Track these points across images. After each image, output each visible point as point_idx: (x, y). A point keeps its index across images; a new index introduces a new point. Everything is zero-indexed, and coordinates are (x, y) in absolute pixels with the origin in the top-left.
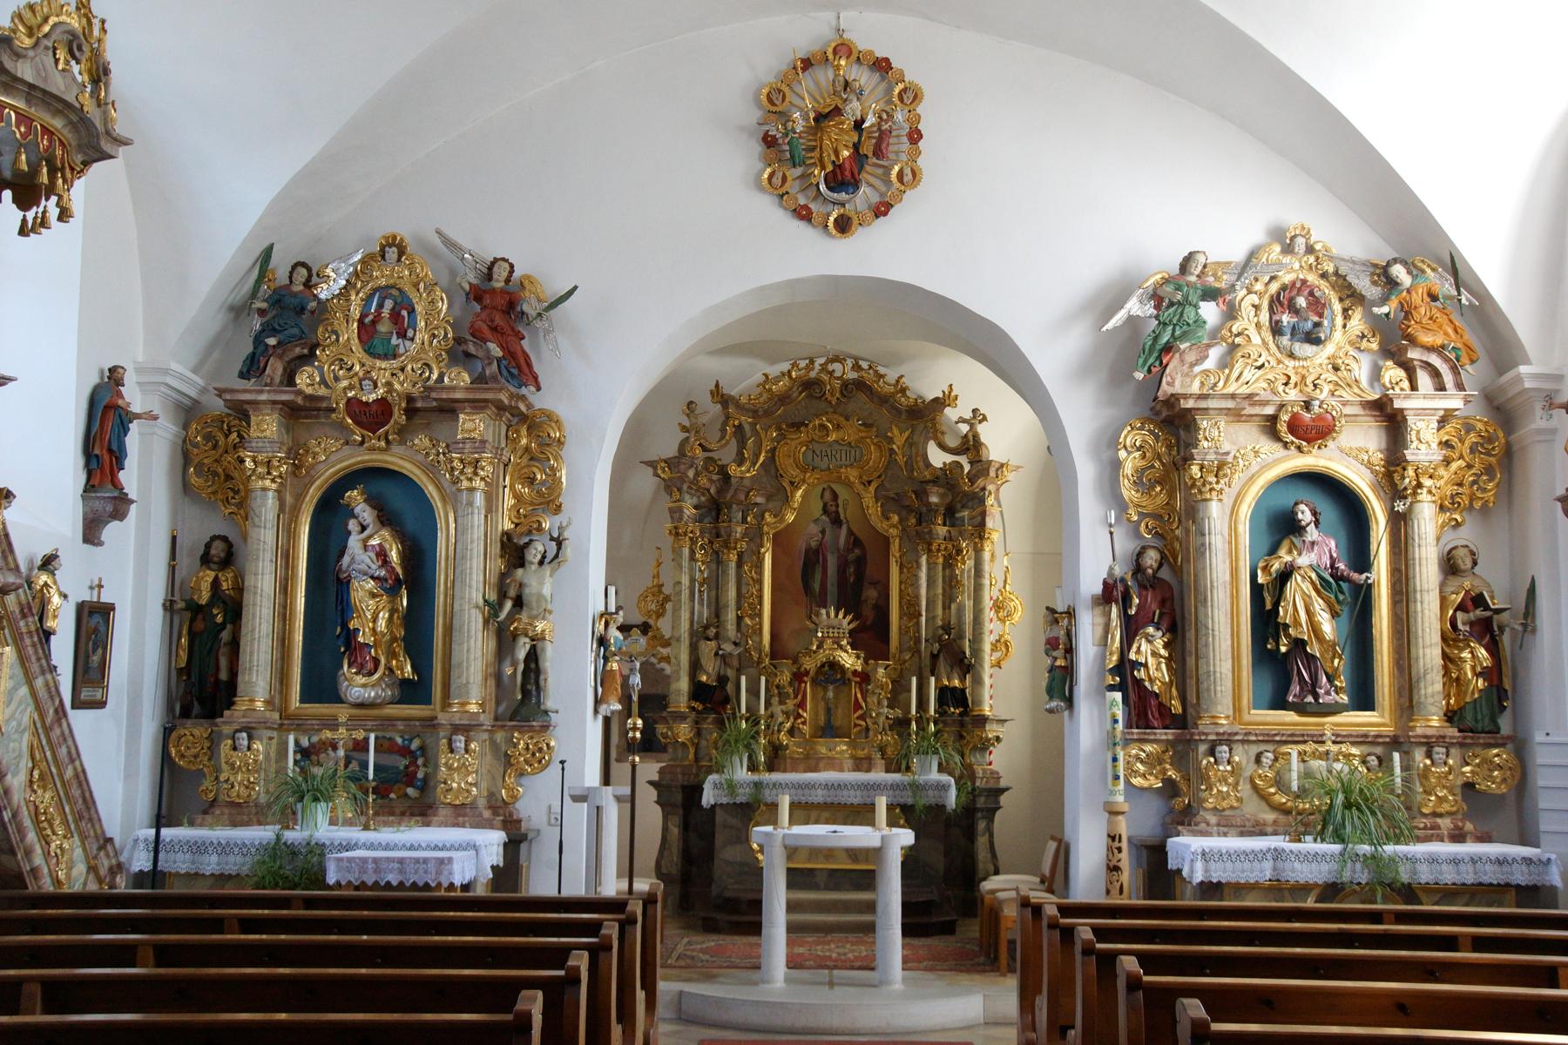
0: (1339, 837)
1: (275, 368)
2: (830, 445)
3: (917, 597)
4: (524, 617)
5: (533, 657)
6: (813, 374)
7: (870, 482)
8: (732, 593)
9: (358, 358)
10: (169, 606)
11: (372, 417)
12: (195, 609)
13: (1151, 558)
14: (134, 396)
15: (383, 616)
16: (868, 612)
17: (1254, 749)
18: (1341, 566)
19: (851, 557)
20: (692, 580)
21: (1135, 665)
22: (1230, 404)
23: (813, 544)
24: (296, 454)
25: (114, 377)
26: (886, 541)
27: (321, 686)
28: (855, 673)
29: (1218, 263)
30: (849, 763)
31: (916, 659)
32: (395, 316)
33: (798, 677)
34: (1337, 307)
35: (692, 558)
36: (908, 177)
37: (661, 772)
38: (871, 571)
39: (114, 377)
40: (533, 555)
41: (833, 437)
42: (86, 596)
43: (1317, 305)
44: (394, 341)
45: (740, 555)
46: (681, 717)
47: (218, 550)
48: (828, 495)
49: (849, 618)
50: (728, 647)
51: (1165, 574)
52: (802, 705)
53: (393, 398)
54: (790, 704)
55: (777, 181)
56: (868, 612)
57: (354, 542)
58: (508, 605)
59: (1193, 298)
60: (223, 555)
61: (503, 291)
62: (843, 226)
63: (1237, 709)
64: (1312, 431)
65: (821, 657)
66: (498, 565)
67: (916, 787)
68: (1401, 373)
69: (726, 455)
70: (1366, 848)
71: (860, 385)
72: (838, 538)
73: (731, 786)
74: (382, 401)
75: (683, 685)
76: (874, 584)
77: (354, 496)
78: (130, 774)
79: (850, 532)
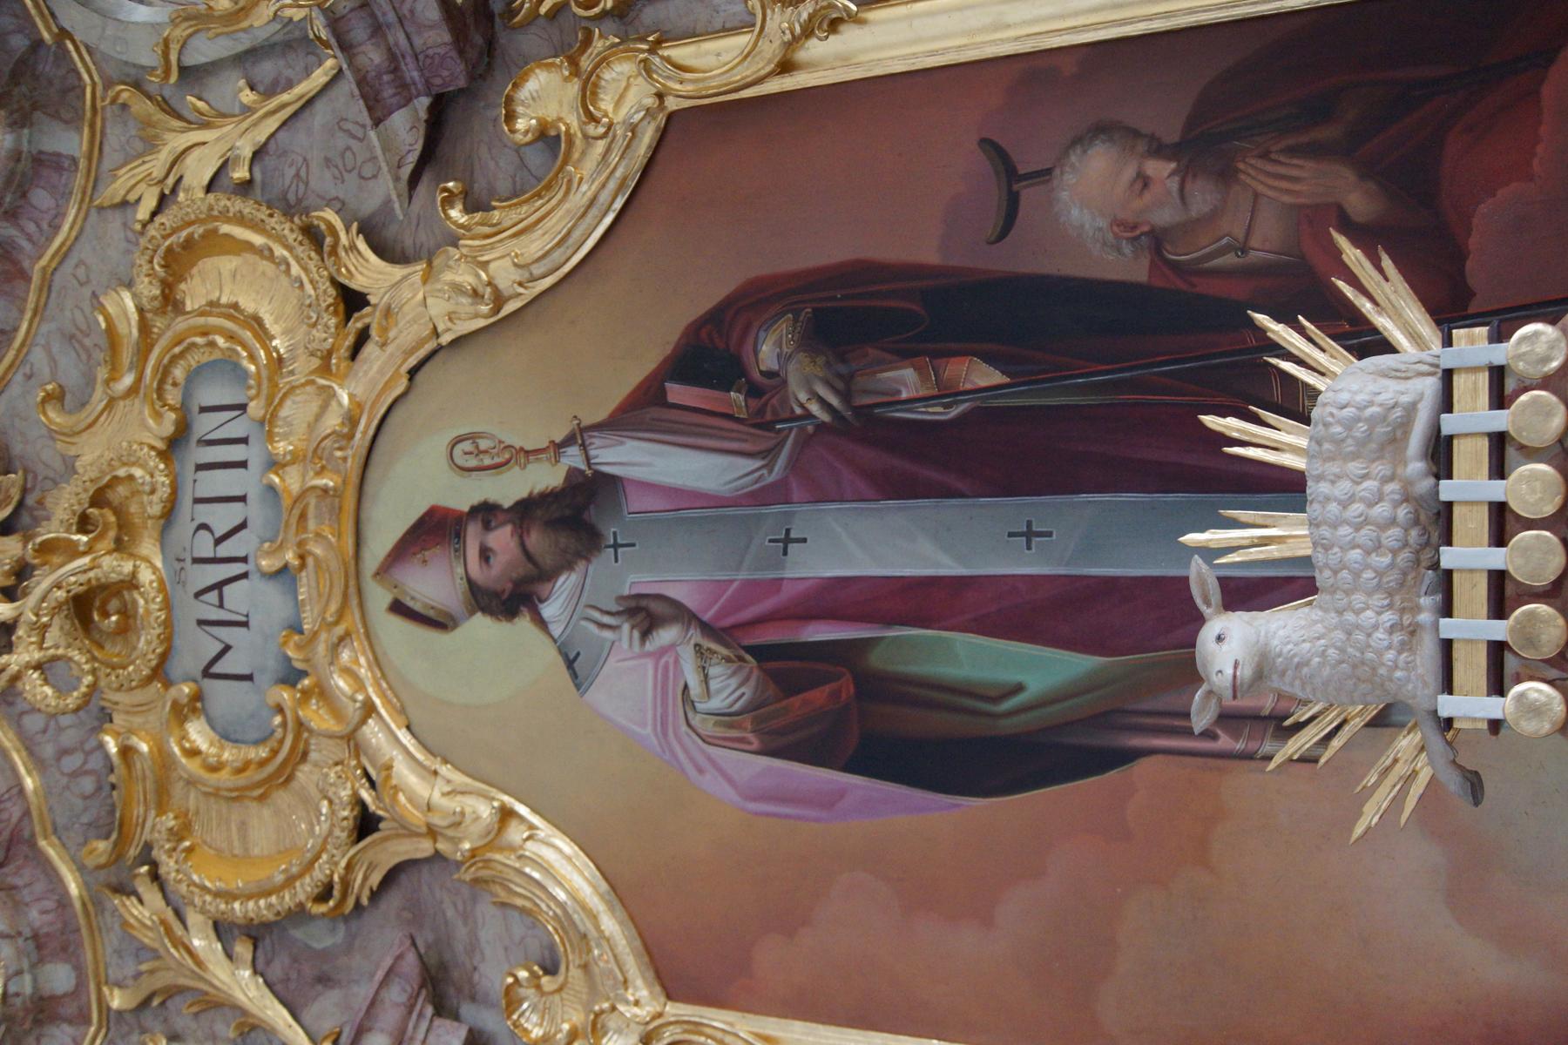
2: (178, 563)
7: (352, 301)
19: (810, 393)
23: (726, 687)
26: (688, 131)
38: (913, 224)
41: (148, 566)
48: (433, 582)
49: (1299, 345)
72: (685, 499)
76: (1013, 181)
79: (642, 411)
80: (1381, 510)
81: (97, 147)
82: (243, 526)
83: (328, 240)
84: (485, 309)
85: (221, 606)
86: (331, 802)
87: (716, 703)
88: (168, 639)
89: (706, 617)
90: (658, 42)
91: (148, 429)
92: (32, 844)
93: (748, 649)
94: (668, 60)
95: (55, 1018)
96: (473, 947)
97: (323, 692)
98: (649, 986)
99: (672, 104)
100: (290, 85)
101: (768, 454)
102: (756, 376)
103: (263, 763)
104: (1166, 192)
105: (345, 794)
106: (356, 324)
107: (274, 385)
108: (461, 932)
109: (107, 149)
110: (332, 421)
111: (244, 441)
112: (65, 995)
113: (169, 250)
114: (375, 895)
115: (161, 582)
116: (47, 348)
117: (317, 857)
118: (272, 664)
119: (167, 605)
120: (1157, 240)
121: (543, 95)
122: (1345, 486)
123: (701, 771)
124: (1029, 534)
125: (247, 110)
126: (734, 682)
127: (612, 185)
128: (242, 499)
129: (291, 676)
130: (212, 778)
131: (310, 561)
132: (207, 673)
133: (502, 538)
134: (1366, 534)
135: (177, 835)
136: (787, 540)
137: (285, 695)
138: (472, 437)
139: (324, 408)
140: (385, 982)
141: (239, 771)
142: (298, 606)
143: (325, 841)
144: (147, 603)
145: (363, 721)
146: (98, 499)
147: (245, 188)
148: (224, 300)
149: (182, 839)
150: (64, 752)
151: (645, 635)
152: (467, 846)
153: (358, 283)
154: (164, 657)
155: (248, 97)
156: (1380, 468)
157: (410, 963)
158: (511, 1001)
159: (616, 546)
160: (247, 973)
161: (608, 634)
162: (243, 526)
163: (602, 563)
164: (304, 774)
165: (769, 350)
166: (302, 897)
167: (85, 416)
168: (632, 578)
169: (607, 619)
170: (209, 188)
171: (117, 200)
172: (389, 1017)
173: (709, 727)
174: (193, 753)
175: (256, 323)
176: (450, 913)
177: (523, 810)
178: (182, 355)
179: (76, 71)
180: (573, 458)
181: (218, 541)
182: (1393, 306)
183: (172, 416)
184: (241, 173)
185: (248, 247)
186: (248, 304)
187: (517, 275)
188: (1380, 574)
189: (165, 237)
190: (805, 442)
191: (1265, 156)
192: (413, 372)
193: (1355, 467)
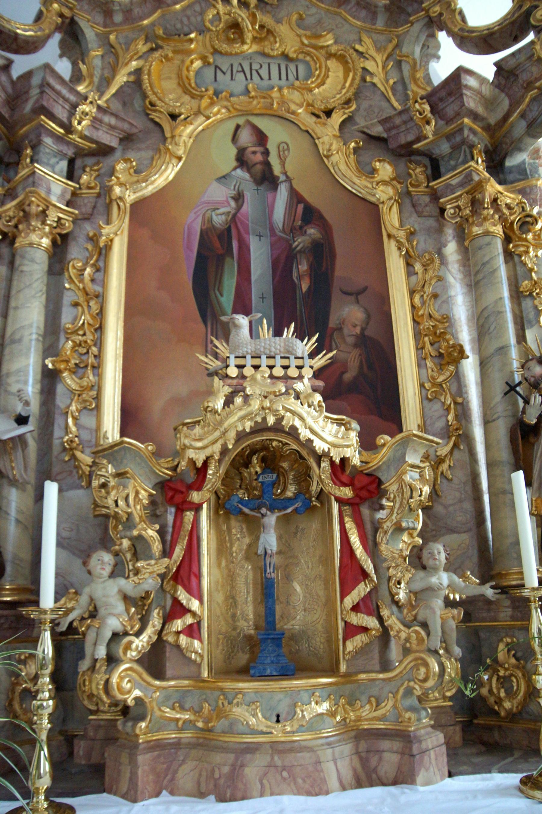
2: (249, 57)
3: (447, 319)
7: (328, 113)
19: (300, 242)
23: (219, 220)
26: (373, 210)
28: (340, 468)
30: (338, 761)
31: (461, 455)
33: (174, 493)
41: (249, 48)
45: (61, 244)
48: (246, 137)
52: (186, 574)
54: (149, 574)
76: (356, 294)
79: (295, 197)
80: (273, 349)
81: (379, 32)
82: (262, 79)
83: (346, 106)
84: (325, 152)
85: (238, 72)
86: (180, 106)
87: (214, 217)
88: (227, 54)
89: (238, 214)
90: (398, 203)
91: (292, 47)
92: (159, 8)
93: (230, 226)
94: (393, 204)
95: (105, 17)
96: (140, 150)
97: (212, 104)
98: (134, 199)
99: (381, 206)
100: (394, 95)
101: (284, 231)
102: (305, 228)
103: (190, 85)
104: (351, 332)
105: (183, 110)
106: (322, 114)
107: (304, 89)
108: (143, 146)
109: (378, 35)
110: (293, 107)
111: (287, 79)
112: (112, 20)
113: (345, 56)
114: (152, 120)
115: (244, 52)
116: (316, 13)
117: (163, 102)
118: (221, 87)
119: (237, 54)
120: (340, 329)
121: (385, 170)
122: (278, 342)
123: (195, 213)
124: (263, 298)
125: (387, 81)
126: (221, 222)
127: (359, 189)
128: (270, 79)
129: (217, 93)
130: (184, 69)
131: (251, 100)
132: (216, 67)
133: (259, 157)
134: (268, 347)
135: (166, 57)
136: (260, 236)
137: (211, 92)
138: (288, 149)
139: (297, 105)
140: (130, 123)
141: (187, 78)
142: (238, 96)
143: (168, 104)
144: (237, 48)
145: (204, 116)
146: (269, 32)
147: (364, 80)
148: (330, 73)
149: (165, 58)
150: (188, 18)
151: (233, 198)
152: (170, 147)
153: (334, 115)
154: (221, 53)
155: (391, 82)
156: (282, 350)
157: (134, 131)
158: (126, 161)
159: (258, 190)
160: (125, 79)
161: (232, 188)
162: (262, 79)
163: (253, 186)
164: (187, 98)
165: (312, 231)
166: (151, 97)
167: (295, 27)
168: (249, 194)
169: (237, 187)
170: (364, 69)
171: (362, 38)
172: (120, 124)
173: (208, 215)
174: (192, 62)
175: (323, 83)
176: (148, 142)
177: (181, 164)
178: (313, 59)
179: (402, 26)
180: (282, 178)
181: (257, 71)
182: (320, 361)
183: (295, 56)
184: (368, 79)
185: (345, 82)
186: (328, 81)
187: (334, 162)
188: (259, 349)
189: (349, 55)
190: (287, 241)
191: (360, 355)
192: (307, 132)
193: (282, 344)
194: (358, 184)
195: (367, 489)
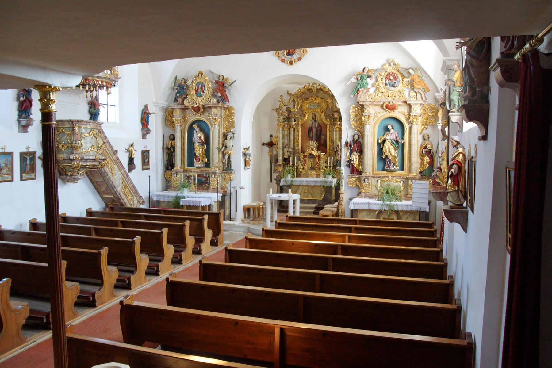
0: (383, 201)
1: (180, 100)
4: (227, 150)
5: (229, 158)
6: (310, 87)
8: (292, 138)
9: (195, 97)
10: (163, 148)
11: (197, 110)
12: (167, 148)
13: (356, 137)
14: (151, 109)
15: (201, 150)
16: (322, 142)
17: (376, 179)
18: (398, 138)
20: (283, 135)
21: (351, 160)
22: (370, 103)
24: (184, 117)
25: (146, 107)
27: (191, 164)
29: (372, 69)
32: (202, 88)
33: (305, 157)
34: (401, 78)
35: (283, 129)
36: (305, 51)
37: (277, 177)
38: (323, 133)
39: (146, 107)
40: (229, 137)
42: (144, 149)
43: (395, 78)
44: (202, 93)
46: (280, 165)
47: (172, 137)
50: (290, 150)
51: (360, 140)
52: (305, 163)
53: (200, 106)
54: (303, 163)
55: (277, 54)
56: (322, 142)
57: (195, 135)
58: (224, 148)
59: (365, 78)
60: (173, 138)
61: (222, 82)
62: (291, 63)
63: (373, 170)
64: (391, 108)
65: (309, 152)
66: (221, 140)
67: (326, 182)
68: (415, 94)
69: (291, 106)
70: (388, 203)
71: (321, 89)
73: (286, 181)
74: (198, 107)
75: (280, 158)
76: (324, 135)
77: (195, 126)
78: (157, 181)
194: (325, 121)
195: (319, 157)
